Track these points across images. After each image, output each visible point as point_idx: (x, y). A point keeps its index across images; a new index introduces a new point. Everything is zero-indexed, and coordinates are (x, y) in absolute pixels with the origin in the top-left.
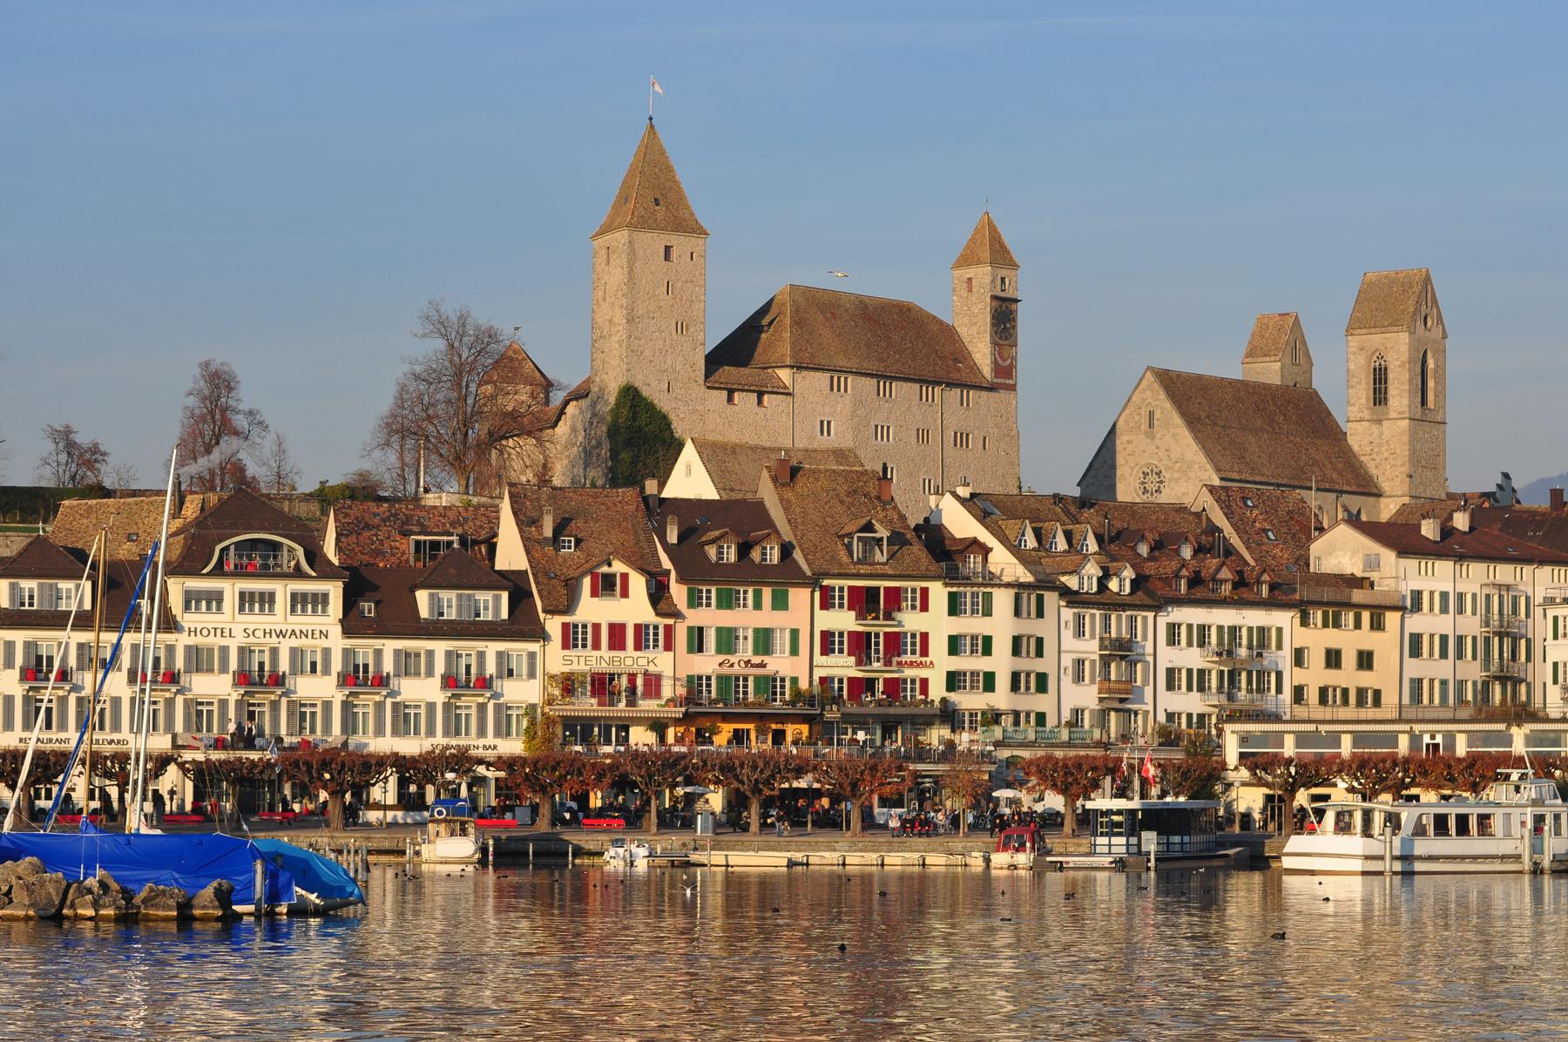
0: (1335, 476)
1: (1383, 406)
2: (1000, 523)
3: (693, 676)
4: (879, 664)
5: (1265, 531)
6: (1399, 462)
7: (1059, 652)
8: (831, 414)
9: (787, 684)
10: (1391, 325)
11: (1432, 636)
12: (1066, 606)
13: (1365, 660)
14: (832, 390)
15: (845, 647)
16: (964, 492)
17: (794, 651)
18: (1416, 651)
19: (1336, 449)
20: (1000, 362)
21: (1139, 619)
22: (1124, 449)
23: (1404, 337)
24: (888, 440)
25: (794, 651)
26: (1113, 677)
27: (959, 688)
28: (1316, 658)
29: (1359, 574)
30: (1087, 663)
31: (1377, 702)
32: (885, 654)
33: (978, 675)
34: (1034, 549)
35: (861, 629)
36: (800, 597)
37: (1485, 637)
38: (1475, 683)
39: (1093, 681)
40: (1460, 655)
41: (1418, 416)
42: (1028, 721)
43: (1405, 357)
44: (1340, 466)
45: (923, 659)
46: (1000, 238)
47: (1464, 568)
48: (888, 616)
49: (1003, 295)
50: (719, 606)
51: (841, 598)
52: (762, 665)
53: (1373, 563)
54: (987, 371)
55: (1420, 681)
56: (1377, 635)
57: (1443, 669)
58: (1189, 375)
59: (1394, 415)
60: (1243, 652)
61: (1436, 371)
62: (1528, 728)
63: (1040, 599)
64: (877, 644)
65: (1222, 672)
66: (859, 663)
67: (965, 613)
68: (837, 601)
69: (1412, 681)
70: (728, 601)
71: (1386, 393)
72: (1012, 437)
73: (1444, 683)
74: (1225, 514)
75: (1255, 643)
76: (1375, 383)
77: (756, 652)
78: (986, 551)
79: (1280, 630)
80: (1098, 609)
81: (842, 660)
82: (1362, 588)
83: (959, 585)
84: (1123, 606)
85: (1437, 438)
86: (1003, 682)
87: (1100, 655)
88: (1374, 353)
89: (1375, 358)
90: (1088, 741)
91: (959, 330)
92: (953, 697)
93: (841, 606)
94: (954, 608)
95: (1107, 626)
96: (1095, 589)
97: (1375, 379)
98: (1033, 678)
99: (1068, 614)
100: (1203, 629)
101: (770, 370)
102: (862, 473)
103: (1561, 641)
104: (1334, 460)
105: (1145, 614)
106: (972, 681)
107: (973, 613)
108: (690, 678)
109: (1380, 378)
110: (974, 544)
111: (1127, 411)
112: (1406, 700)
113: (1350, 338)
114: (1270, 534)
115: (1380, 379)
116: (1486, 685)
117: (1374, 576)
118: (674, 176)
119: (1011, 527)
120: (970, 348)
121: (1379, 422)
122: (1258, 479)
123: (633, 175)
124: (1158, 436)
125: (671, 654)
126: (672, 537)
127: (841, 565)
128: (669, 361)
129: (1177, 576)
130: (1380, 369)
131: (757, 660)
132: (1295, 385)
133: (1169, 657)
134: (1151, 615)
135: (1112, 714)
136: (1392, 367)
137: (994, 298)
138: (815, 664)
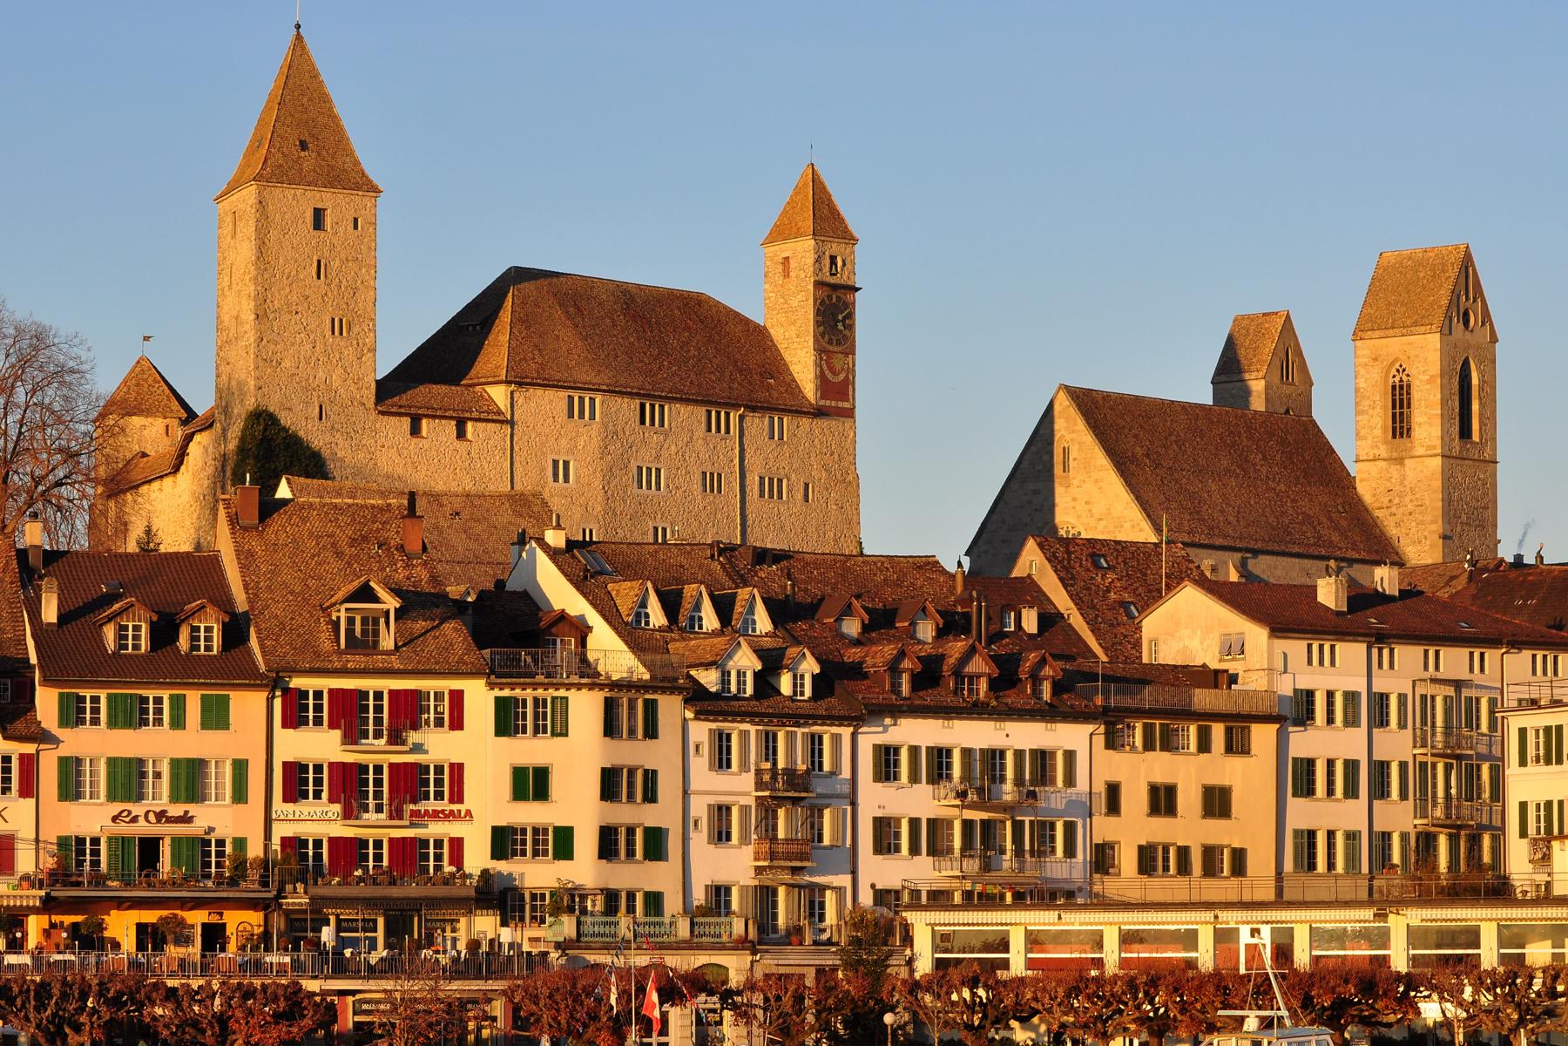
0: (1335, 538)
1: (1405, 439)
2: (610, 587)
3: (67, 838)
4: (383, 816)
5: (1123, 604)
6: (1429, 518)
7: (686, 793)
8: (570, 451)
9: (228, 849)
10: (1415, 324)
11: (1330, 763)
12: (696, 718)
13: (1217, 802)
14: (571, 415)
15: (325, 787)
16: (555, 538)
17: (240, 795)
18: (1305, 787)
19: (1340, 501)
20: (827, 372)
21: (826, 740)
22: (1029, 502)
23: (1434, 340)
24: (659, 488)
25: (240, 795)
26: (781, 834)
27: (514, 853)
28: (1135, 799)
29: (1214, 665)
30: (735, 811)
31: (1239, 867)
32: (391, 799)
33: (545, 831)
34: (661, 629)
35: (350, 758)
36: (248, 706)
37: (1420, 763)
38: (1404, 837)
39: (745, 840)
40: (1380, 789)
41: (1456, 451)
42: (631, 909)
43: (1435, 368)
44: (1344, 523)
45: (455, 807)
46: (830, 199)
47: (1386, 652)
48: (396, 738)
49: (832, 280)
50: (113, 723)
51: (318, 708)
52: (186, 819)
53: (1234, 648)
54: (809, 389)
55: (1312, 834)
56: (1237, 762)
57: (1349, 815)
58: (1122, 397)
59: (1420, 451)
60: (1008, 791)
61: (1481, 388)
62: (1416, 916)
63: (651, 708)
64: (378, 783)
65: (968, 825)
66: (348, 814)
67: (524, 732)
68: (311, 714)
69: (1297, 833)
70: (132, 715)
71: (1409, 422)
72: (846, 483)
73: (1352, 836)
74: (1061, 580)
75: (1027, 777)
76: (1394, 407)
77: (174, 798)
78: (582, 630)
79: (1070, 756)
80: (752, 722)
81: (319, 810)
82: (1216, 686)
83: (512, 687)
84: (798, 718)
85: (1484, 484)
86: (586, 843)
87: (758, 798)
88: (1392, 364)
89: (1394, 372)
90: (725, 938)
91: (772, 332)
92: (502, 867)
93: (318, 722)
94: (507, 721)
95: (769, 750)
96: (749, 691)
97: (1394, 402)
98: (639, 836)
99: (701, 731)
100: (940, 757)
101: (478, 388)
102: (381, 509)
103: (1532, 768)
104: (1334, 516)
105: (835, 730)
106: (535, 842)
107: (536, 731)
108: (63, 842)
109: (1400, 399)
110: (562, 616)
111: (1033, 448)
112: (1288, 865)
113: (1359, 343)
114: (1132, 607)
115: (1401, 401)
116: (1426, 841)
117: (1232, 667)
118: (331, 108)
119: (624, 593)
120: (787, 357)
121: (1400, 461)
122: (1219, 541)
123: (271, 108)
124: (1075, 482)
125: (32, 802)
126: (50, 613)
127: (317, 654)
128: (321, 375)
129: (894, 668)
130: (1401, 387)
131: (176, 810)
132: (1287, 412)
133: (875, 799)
134: (846, 732)
135: (781, 891)
136: (1418, 383)
137: (819, 284)
138: (274, 816)
